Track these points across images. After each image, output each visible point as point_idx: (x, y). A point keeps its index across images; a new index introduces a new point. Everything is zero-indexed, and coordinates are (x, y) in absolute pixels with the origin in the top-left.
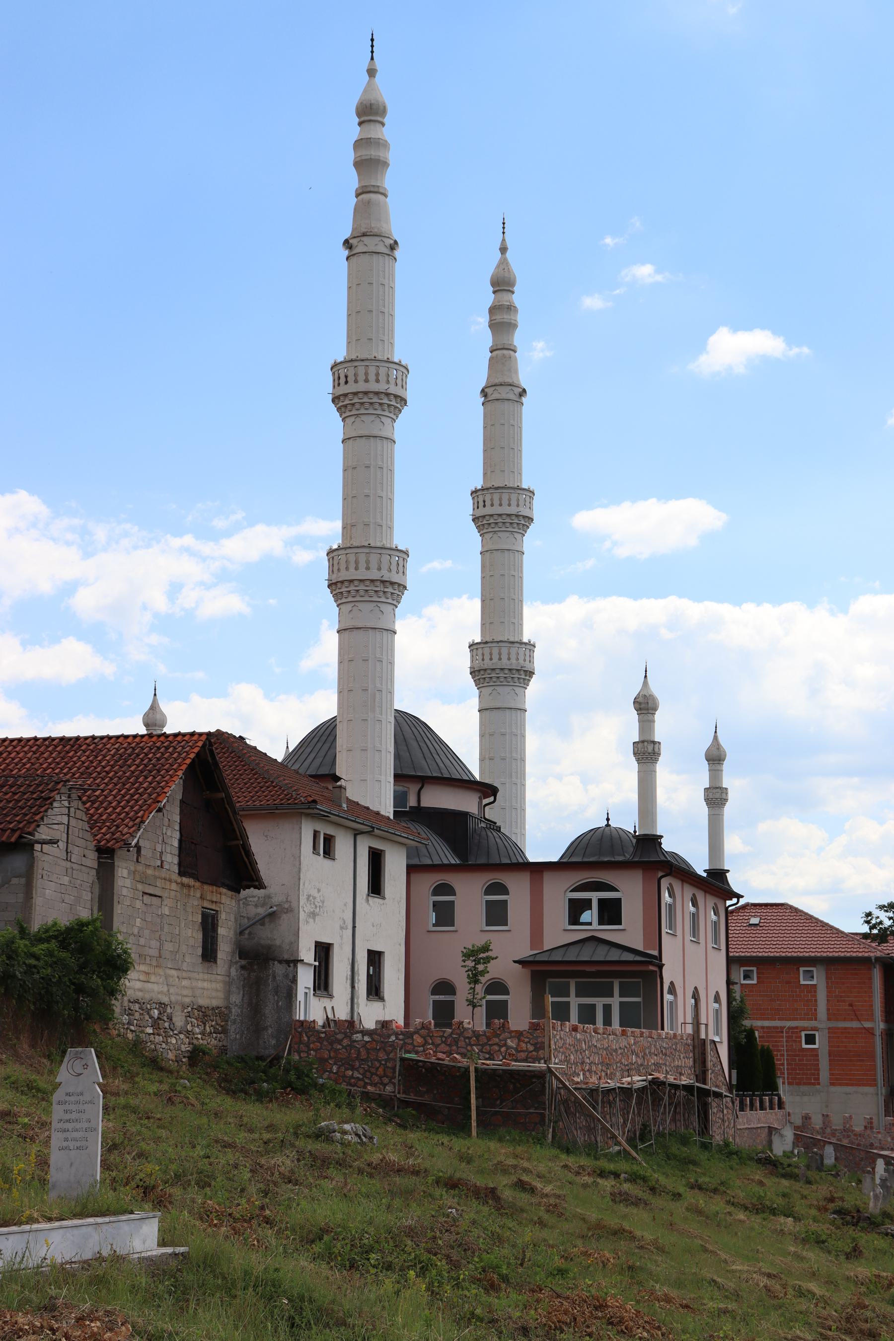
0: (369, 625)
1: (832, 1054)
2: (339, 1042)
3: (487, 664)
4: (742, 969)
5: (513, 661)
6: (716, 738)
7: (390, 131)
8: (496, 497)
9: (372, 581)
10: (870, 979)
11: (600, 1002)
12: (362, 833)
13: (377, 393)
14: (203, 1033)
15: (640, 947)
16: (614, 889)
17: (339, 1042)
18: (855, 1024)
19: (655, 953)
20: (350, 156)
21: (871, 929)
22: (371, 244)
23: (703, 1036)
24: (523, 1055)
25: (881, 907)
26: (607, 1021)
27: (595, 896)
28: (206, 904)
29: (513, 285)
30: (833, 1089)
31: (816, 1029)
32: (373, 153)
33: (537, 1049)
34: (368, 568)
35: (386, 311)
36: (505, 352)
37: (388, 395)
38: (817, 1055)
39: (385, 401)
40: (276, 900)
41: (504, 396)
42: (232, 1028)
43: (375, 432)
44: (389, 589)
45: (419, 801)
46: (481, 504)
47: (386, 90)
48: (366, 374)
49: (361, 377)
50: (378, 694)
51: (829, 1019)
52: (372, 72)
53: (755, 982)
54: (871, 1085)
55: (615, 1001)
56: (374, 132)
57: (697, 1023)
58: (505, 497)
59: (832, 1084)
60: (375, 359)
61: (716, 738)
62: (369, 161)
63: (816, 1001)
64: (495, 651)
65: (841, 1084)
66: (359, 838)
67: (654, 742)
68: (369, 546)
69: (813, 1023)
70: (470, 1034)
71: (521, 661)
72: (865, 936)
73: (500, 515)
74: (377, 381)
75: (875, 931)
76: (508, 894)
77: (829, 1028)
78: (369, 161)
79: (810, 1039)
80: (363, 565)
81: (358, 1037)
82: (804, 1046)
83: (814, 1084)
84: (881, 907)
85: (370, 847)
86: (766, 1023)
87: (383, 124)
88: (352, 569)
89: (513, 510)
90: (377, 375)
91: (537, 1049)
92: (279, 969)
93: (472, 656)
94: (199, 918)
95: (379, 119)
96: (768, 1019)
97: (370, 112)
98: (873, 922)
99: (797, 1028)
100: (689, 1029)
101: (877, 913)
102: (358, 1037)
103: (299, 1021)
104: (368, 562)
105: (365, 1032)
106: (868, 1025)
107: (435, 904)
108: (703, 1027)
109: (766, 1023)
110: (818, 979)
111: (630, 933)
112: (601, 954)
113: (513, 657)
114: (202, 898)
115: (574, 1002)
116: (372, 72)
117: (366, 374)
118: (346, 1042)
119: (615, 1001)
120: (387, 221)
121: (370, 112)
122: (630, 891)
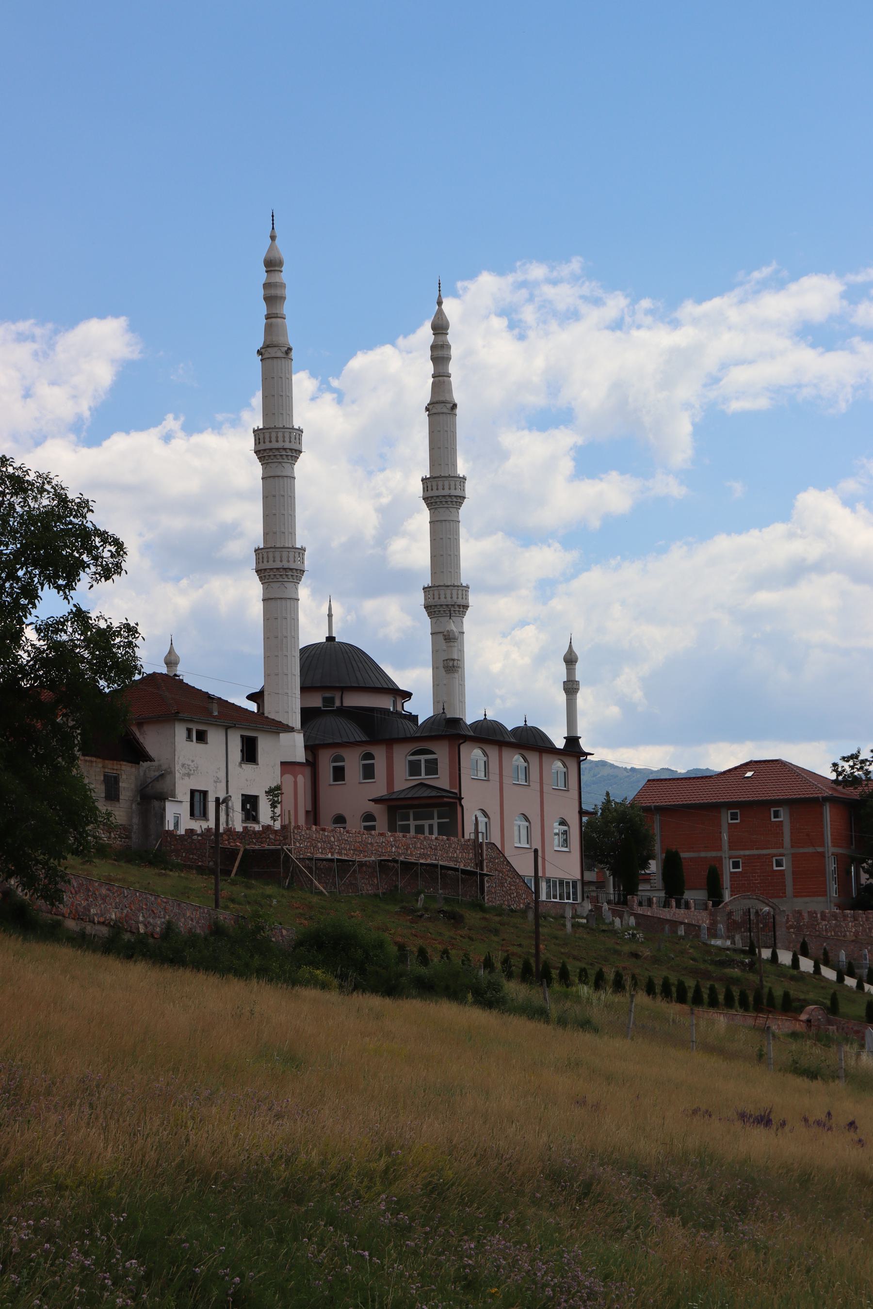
0: (277, 596)
1: (794, 873)
2: (186, 840)
3: (436, 601)
4: (729, 812)
5: (442, 599)
6: (570, 646)
7: (286, 275)
8: (434, 484)
9: (278, 569)
10: (822, 814)
11: (426, 823)
12: (231, 727)
13: (278, 449)
14: (109, 838)
15: (447, 788)
16: (432, 753)
17: (186, 840)
18: (811, 850)
19: (456, 791)
20: (261, 292)
21: (838, 775)
22: (272, 352)
23: (481, 840)
24: (278, 842)
25: (844, 758)
26: (431, 833)
27: (423, 758)
28: (106, 770)
29: (447, 329)
30: (795, 900)
31: (783, 855)
32: (273, 292)
33: (285, 839)
34: (274, 561)
35: (284, 394)
36: (441, 378)
37: (285, 449)
38: (784, 875)
39: (284, 453)
40: (164, 767)
41: (439, 411)
42: (134, 836)
43: (279, 474)
44: (295, 574)
45: (342, 703)
46: (430, 488)
47: (284, 250)
48: (270, 437)
49: (267, 440)
50: (284, 640)
51: (792, 847)
52: (273, 238)
53: (738, 821)
54: (822, 896)
55: (435, 822)
56: (275, 278)
57: (477, 832)
58: (440, 484)
59: (795, 896)
60: (275, 428)
61: (570, 646)
62: (273, 297)
63: (782, 833)
64: (436, 593)
65: (802, 896)
66: (230, 732)
67: (453, 660)
68: (275, 548)
69: (781, 851)
70: (251, 833)
71: (455, 598)
72: (836, 782)
73: (437, 497)
74: (277, 441)
75: (840, 778)
76: (374, 759)
77: (792, 854)
78: (273, 297)
79: (779, 864)
80: (271, 559)
81: (195, 837)
82: (775, 868)
83: (782, 897)
84: (844, 758)
85: (242, 736)
86: (747, 852)
87: (281, 271)
88: (265, 562)
89: (446, 492)
90: (277, 437)
91: (285, 839)
92: (156, 803)
93: (425, 596)
94: (102, 778)
95: (277, 268)
96: (748, 849)
97: (272, 265)
98: (840, 769)
99: (769, 855)
100: (473, 837)
101: (841, 763)
102: (195, 837)
103: (167, 831)
104: (274, 557)
105: (198, 835)
106: (820, 849)
107: (334, 767)
108: (480, 835)
109: (747, 852)
110: (784, 816)
111: (442, 781)
112: (428, 793)
113: (449, 596)
114: (104, 767)
115: (412, 823)
116: (273, 238)
117: (270, 437)
118: (189, 840)
119: (435, 822)
120: (285, 334)
121: (272, 265)
122: (441, 753)
